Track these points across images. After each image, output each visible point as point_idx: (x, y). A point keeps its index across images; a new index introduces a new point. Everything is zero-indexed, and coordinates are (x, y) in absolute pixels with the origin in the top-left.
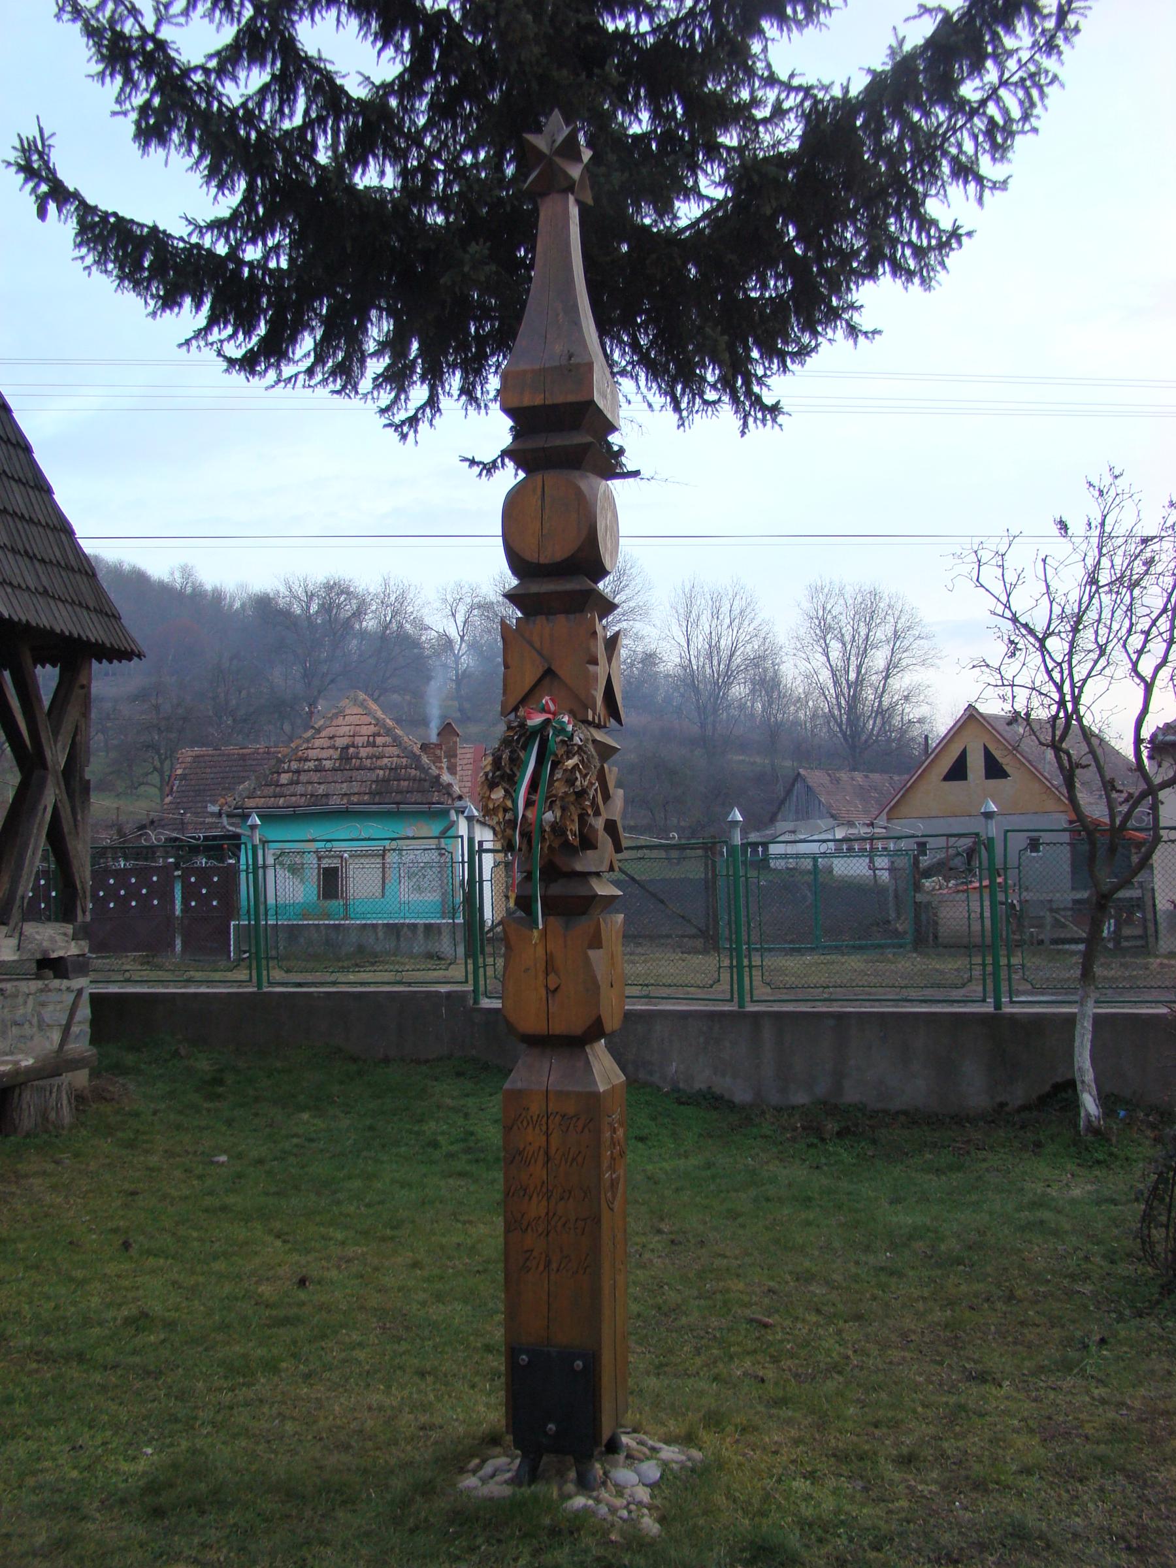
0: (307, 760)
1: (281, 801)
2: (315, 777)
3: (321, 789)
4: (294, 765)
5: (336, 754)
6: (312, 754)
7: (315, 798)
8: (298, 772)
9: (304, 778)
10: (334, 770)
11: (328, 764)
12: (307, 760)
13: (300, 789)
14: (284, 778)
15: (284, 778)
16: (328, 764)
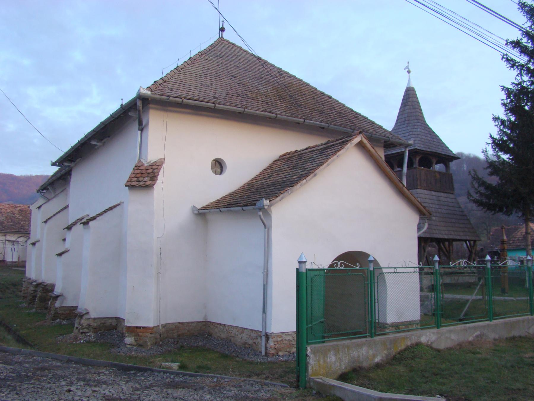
0: (516, 238)
1: (510, 247)
2: (518, 241)
3: (519, 244)
4: (513, 239)
5: (522, 236)
6: (517, 236)
7: (517, 246)
8: (514, 241)
9: (515, 242)
10: (522, 240)
11: (520, 239)
12: (516, 238)
13: (514, 244)
14: (511, 242)
15: (511, 242)
16: (520, 239)
